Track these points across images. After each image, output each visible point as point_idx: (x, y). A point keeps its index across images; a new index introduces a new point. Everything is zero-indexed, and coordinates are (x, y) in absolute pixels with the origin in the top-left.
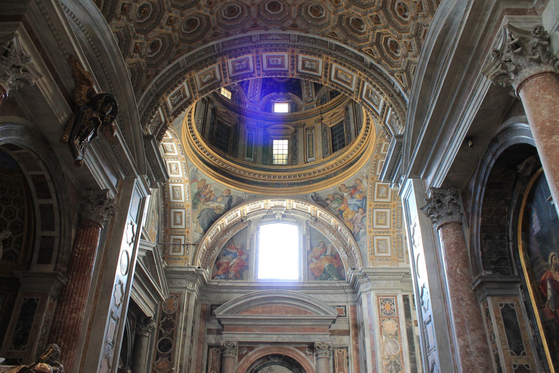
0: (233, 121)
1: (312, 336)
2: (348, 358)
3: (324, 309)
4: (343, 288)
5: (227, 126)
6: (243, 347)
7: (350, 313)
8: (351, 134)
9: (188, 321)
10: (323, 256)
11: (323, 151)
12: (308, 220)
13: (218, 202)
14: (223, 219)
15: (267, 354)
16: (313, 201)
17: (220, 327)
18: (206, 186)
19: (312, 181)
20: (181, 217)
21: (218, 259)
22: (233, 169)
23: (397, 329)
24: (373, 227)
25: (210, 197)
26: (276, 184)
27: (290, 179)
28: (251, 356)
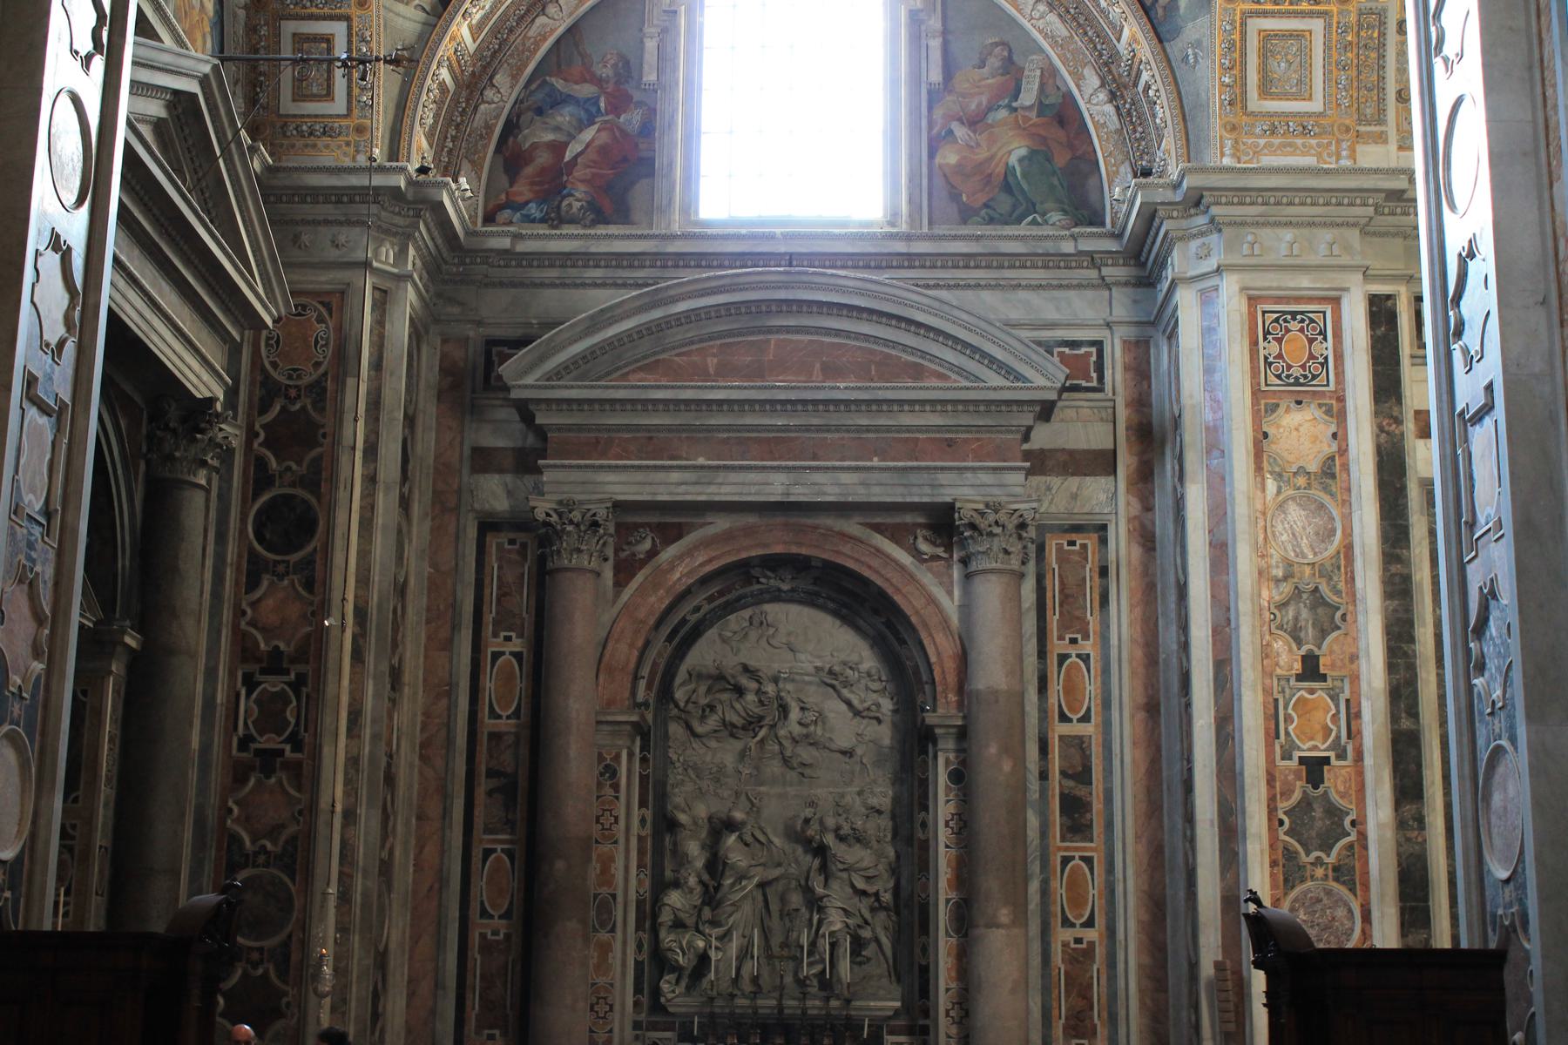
1: (943, 478)
2: (1104, 572)
3: (999, 354)
4: (1093, 259)
6: (637, 526)
7: (1119, 377)
9: (384, 417)
10: (1002, 114)
15: (744, 555)
17: (531, 440)
21: (511, 127)
23: (1335, 447)
28: (672, 568)
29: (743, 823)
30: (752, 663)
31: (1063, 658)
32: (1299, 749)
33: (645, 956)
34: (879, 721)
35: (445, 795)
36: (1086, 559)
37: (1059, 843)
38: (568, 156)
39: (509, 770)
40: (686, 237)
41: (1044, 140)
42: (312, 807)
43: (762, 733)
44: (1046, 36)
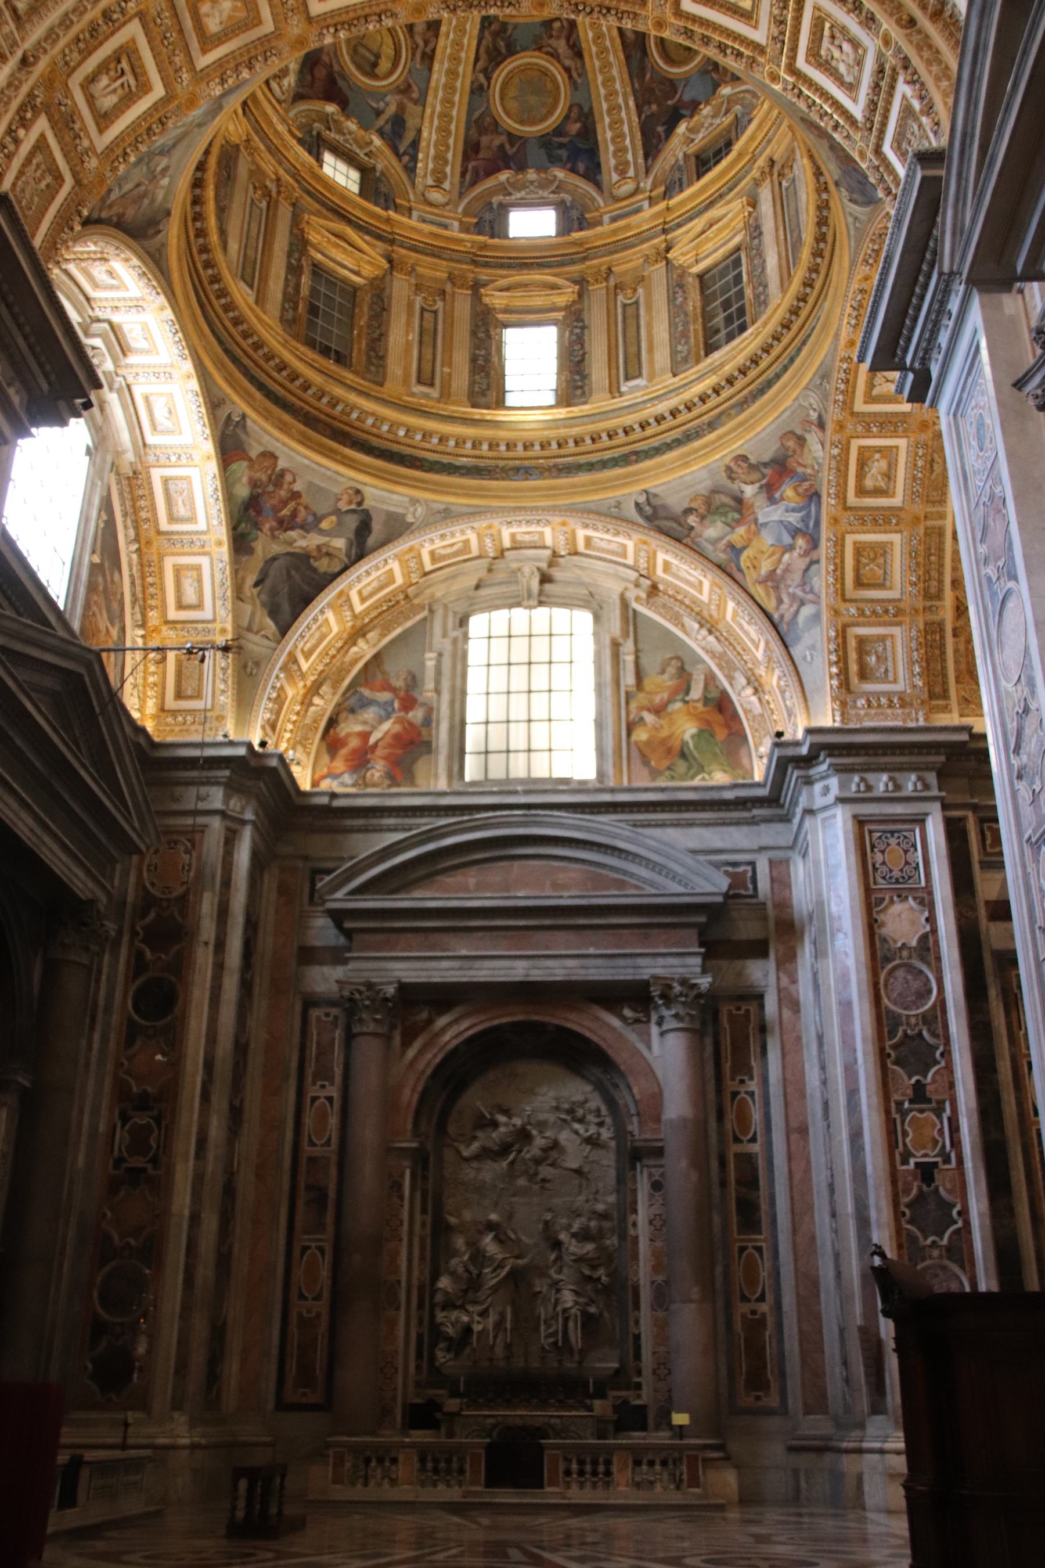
0: (370, 263)
1: (641, 961)
5: (345, 281)
8: (766, 286)
10: (678, 705)
11: (674, 353)
13: (322, 532)
16: (641, 521)
17: (342, 941)
19: (636, 453)
20: (200, 581)
21: (332, 722)
23: (928, 928)
25: (294, 514)
26: (517, 470)
27: (562, 452)
28: (443, 1030)
32: (914, 1156)
36: (749, 1020)
37: (736, 1236)
38: (372, 740)
41: (708, 723)
43: (511, 1157)
44: (707, 652)
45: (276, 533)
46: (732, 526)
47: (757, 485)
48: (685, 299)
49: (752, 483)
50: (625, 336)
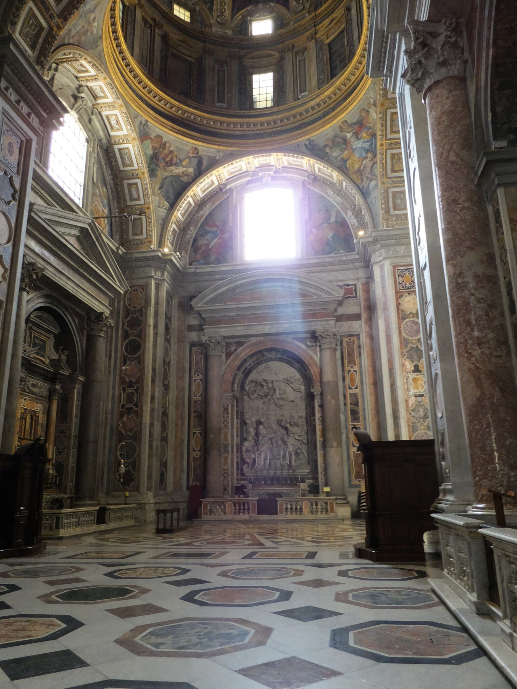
2: (359, 347)
3: (325, 288)
4: (352, 261)
7: (361, 293)
11: (319, 79)
12: (304, 180)
13: (183, 166)
14: (193, 188)
15: (260, 349)
16: (307, 152)
18: (164, 145)
20: (137, 189)
21: (195, 240)
22: (199, 119)
24: (386, 175)
25: (172, 160)
26: (258, 135)
27: (276, 126)
28: (241, 353)
29: (264, 422)
30: (265, 378)
31: (349, 371)
33: (239, 460)
34: (301, 392)
35: (183, 419)
36: (354, 343)
38: (210, 247)
39: (199, 410)
40: (240, 265)
42: (141, 423)
43: (269, 397)
44: (337, 203)
45: (166, 168)
46: (343, 151)
47: (352, 133)
48: (323, 55)
49: (350, 132)
50: (300, 75)
